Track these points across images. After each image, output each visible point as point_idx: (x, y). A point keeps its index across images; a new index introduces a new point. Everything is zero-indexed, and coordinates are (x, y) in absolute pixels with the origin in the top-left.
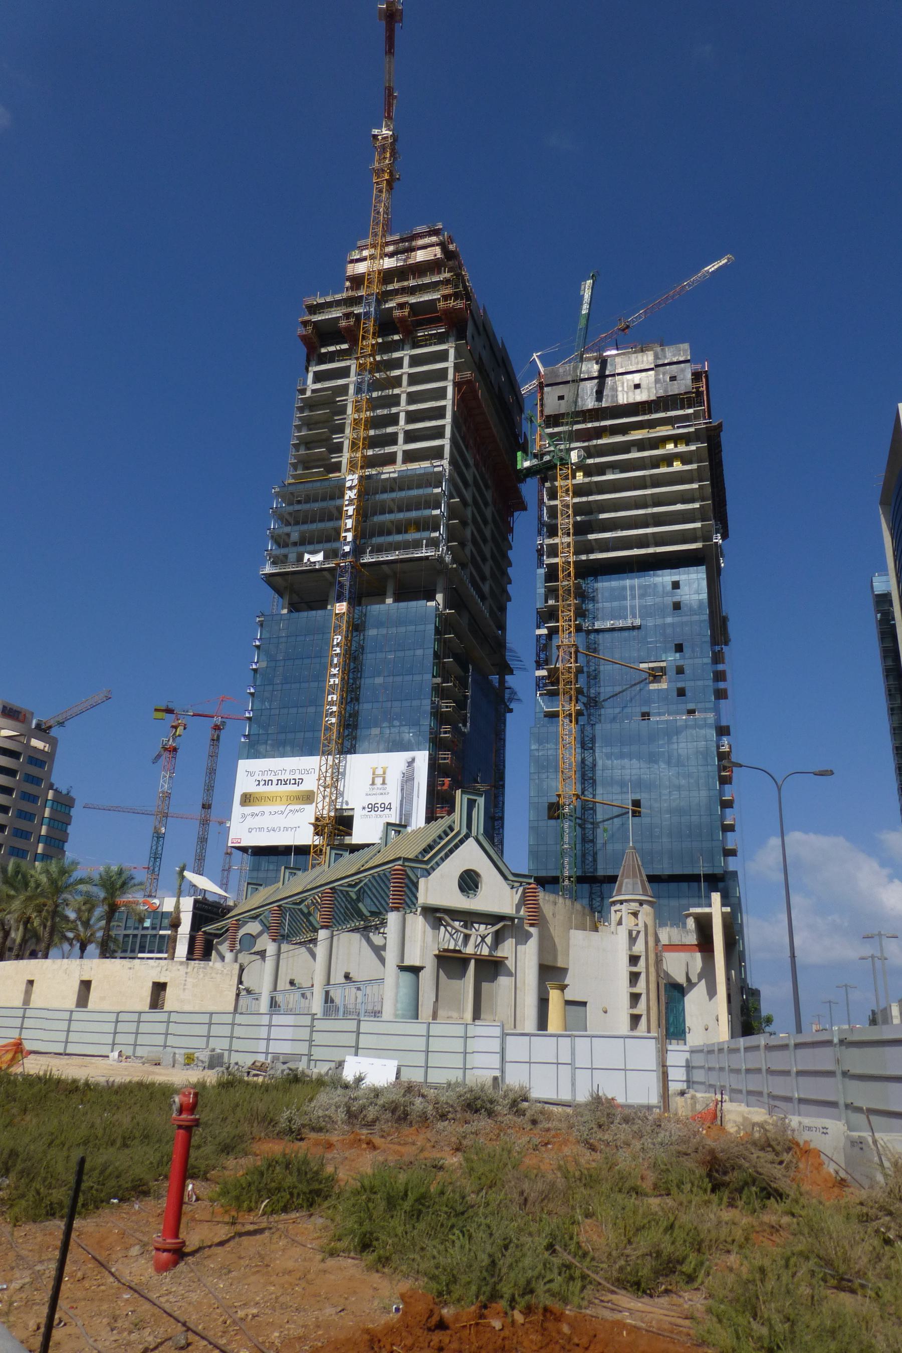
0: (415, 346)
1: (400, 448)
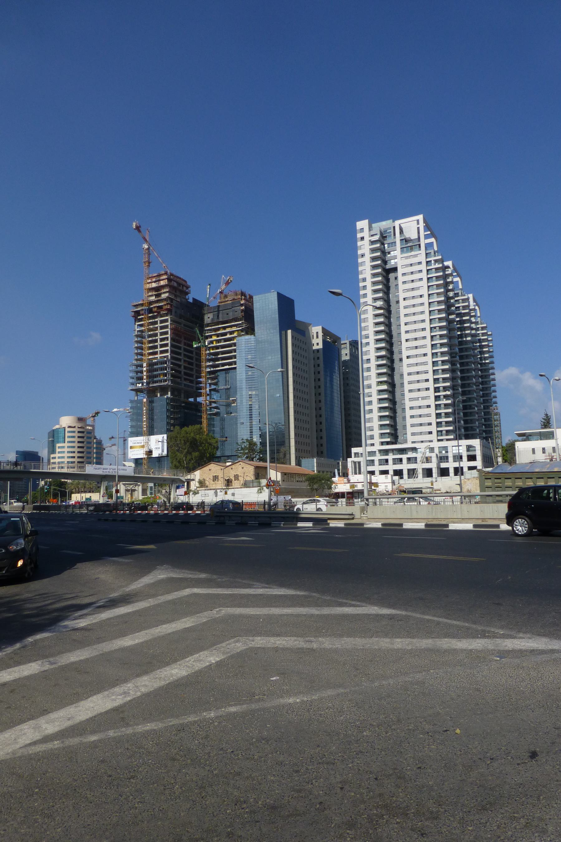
1: (159, 350)
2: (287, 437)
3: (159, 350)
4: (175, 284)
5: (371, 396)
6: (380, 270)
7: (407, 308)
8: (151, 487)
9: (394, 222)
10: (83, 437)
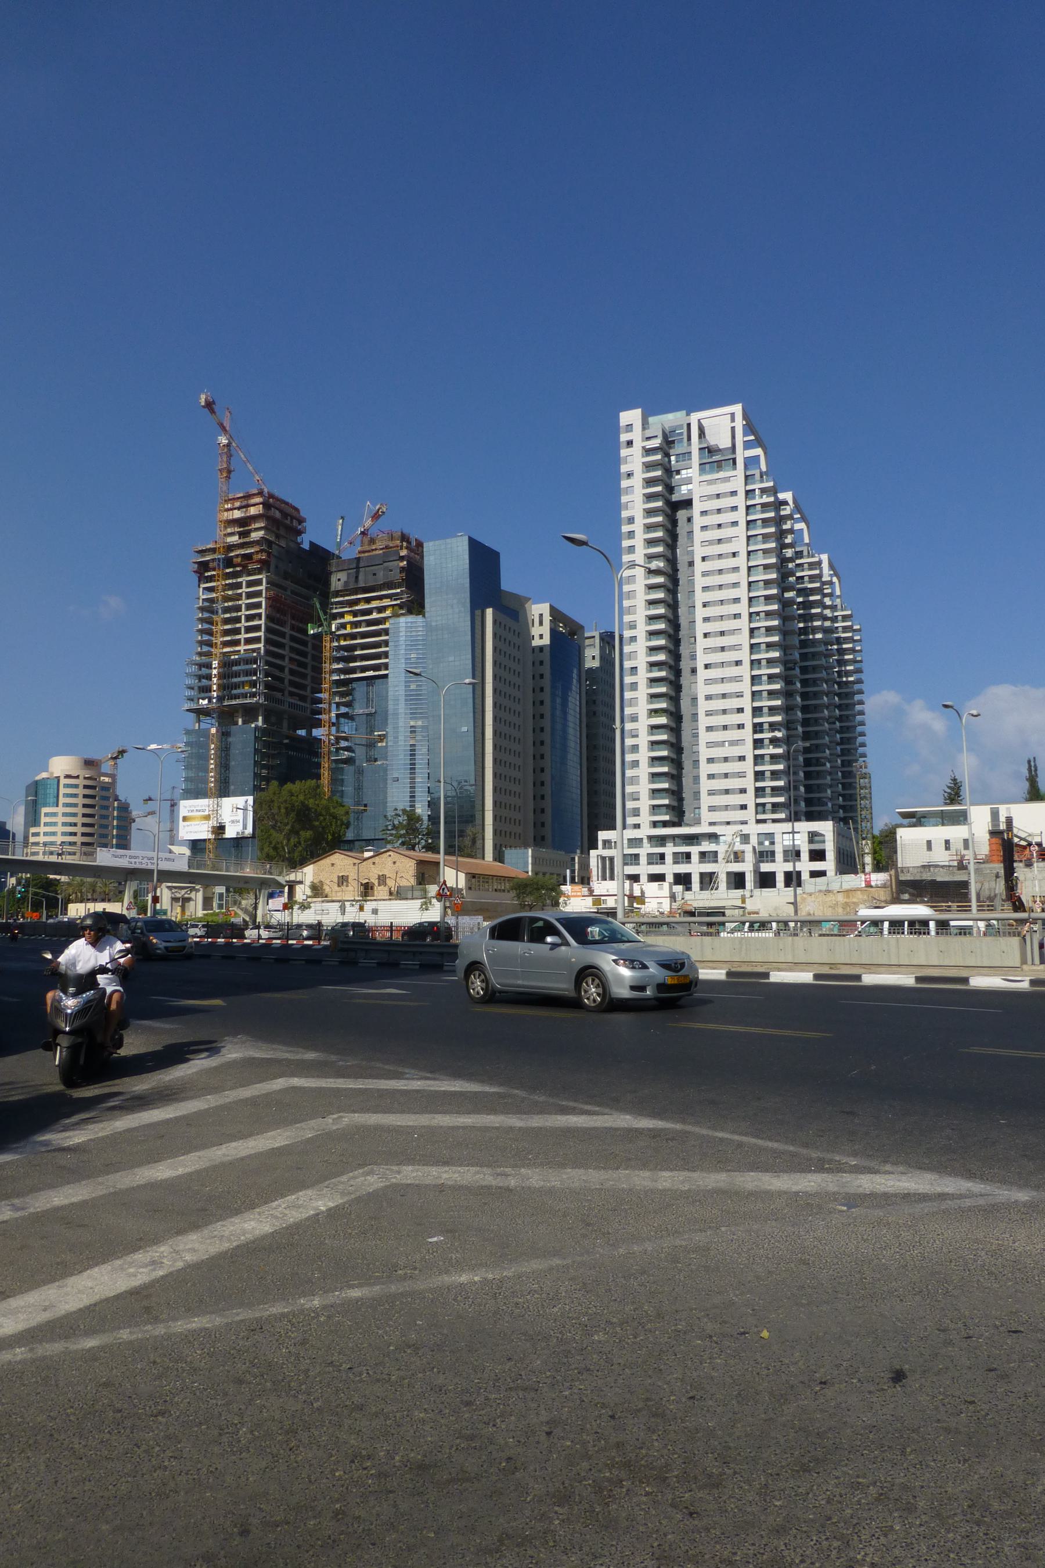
0: (250, 575)
1: (243, 636)
2: (478, 807)
3: (243, 636)
4: (278, 515)
5: (637, 736)
6: (660, 504)
7: (708, 575)
8: (221, 895)
9: (688, 414)
10: (93, 797)
